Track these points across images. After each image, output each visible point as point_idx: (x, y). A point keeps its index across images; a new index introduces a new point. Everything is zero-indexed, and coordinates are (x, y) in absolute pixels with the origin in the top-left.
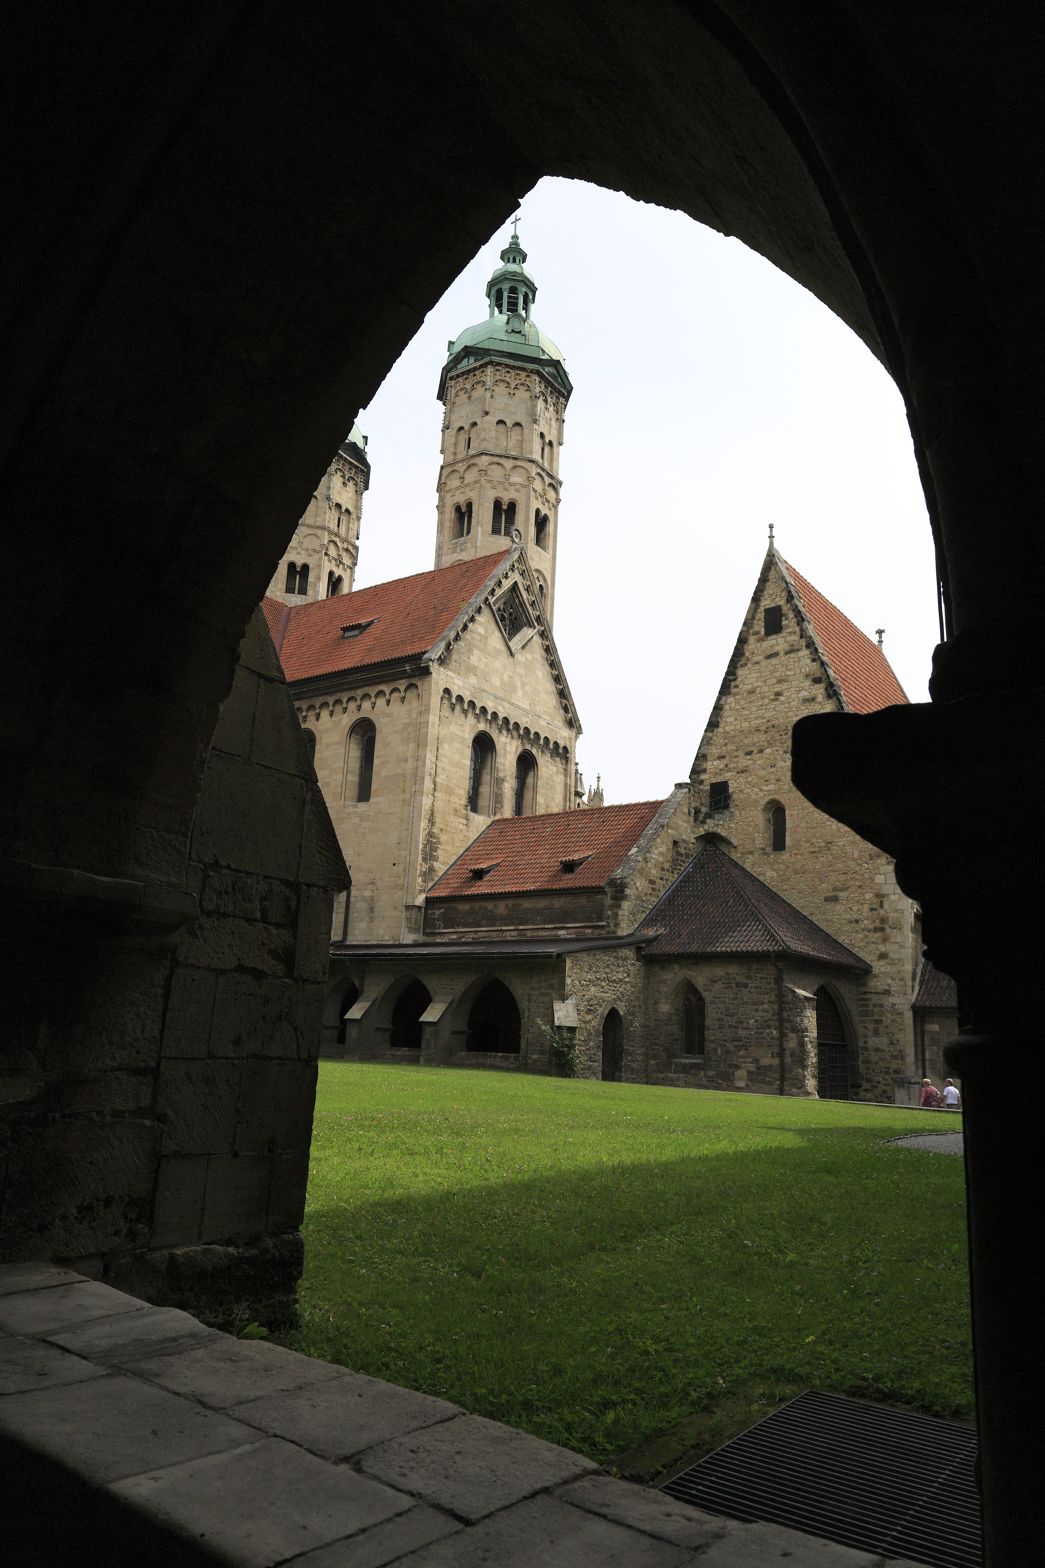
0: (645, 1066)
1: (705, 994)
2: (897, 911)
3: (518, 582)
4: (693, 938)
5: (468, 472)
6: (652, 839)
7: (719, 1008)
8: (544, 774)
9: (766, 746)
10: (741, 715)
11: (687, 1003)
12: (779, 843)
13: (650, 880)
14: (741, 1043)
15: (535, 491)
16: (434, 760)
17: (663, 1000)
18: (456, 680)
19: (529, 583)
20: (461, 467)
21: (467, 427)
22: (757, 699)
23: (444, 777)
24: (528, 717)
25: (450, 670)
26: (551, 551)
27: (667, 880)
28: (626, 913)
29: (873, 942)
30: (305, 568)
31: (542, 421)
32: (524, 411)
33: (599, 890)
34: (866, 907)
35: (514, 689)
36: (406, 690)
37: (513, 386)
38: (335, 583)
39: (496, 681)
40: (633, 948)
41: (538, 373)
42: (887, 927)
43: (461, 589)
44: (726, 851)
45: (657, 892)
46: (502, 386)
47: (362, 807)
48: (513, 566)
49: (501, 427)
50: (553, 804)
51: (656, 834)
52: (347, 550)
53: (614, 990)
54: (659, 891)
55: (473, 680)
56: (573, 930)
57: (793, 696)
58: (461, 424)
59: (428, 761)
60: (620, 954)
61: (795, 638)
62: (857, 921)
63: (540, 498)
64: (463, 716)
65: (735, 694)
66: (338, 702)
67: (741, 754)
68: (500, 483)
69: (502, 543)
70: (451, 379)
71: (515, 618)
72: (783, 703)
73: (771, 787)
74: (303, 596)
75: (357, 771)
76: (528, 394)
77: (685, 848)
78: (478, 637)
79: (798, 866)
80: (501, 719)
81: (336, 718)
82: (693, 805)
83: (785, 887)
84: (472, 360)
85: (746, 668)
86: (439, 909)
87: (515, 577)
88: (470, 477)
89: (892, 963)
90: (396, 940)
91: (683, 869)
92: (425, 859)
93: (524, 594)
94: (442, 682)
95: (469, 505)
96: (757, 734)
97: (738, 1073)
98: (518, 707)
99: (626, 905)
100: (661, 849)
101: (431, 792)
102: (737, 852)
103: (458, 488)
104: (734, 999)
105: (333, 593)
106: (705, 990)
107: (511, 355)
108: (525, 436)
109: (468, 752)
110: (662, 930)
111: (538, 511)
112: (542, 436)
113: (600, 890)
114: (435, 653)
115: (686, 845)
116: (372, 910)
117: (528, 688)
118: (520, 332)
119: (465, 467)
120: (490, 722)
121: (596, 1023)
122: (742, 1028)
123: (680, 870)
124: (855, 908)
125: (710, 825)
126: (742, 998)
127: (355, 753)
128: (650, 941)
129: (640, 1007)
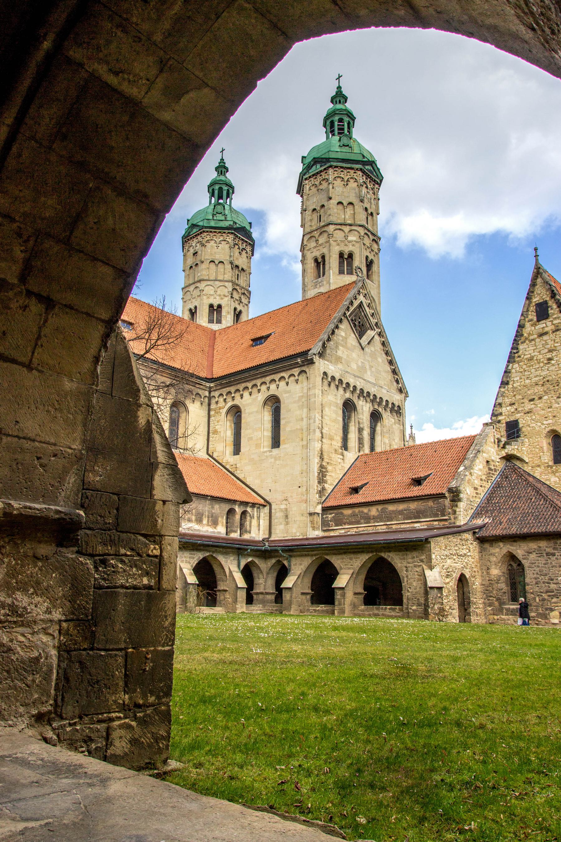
0: (485, 611)
1: (523, 562)
3: (363, 301)
4: (511, 524)
5: (321, 237)
6: (473, 461)
7: (535, 570)
8: (387, 424)
9: (544, 394)
10: (524, 375)
11: (510, 568)
14: (553, 594)
16: (320, 418)
17: (493, 566)
19: (369, 302)
20: (316, 234)
21: (318, 208)
22: (535, 364)
23: (327, 429)
25: (326, 360)
26: (377, 283)
28: (462, 510)
30: (220, 306)
31: (366, 200)
32: (354, 195)
33: (441, 496)
35: (366, 372)
36: (299, 375)
37: (346, 180)
38: (238, 315)
39: (354, 366)
40: (471, 532)
41: (361, 170)
43: (327, 309)
44: (520, 466)
46: (339, 180)
47: (275, 451)
48: (359, 291)
49: (340, 207)
50: (394, 443)
51: (476, 456)
52: (244, 294)
55: (340, 366)
56: (425, 523)
58: (314, 207)
59: (317, 419)
60: (463, 537)
64: (336, 389)
65: (518, 363)
66: (255, 385)
67: (526, 401)
69: (348, 279)
70: (306, 179)
72: (553, 365)
73: (550, 421)
74: (219, 324)
75: (270, 429)
76: (356, 184)
77: (494, 466)
78: (341, 338)
81: (253, 396)
84: (318, 166)
86: (331, 514)
88: (322, 240)
90: (303, 536)
91: (493, 479)
92: (319, 483)
93: (367, 309)
95: (323, 257)
96: (537, 387)
97: (553, 614)
99: (462, 505)
100: (479, 467)
101: (320, 439)
102: (528, 466)
103: (315, 247)
104: (545, 564)
105: (237, 322)
107: (343, 161)
108: (356, 211)
109: (340, 412)
110: (487, 520)
111: (367, 257)
112: (366, 209)
114: (317, 348)
116: (287, 517)
117: (373, 369)
118: (348, 146)
119: (318, 234)
121: (452, 584)
122: (553, 583)
126: (551, 563)
127: (267, 417)
128: (481, 528)
129: (478, 572)
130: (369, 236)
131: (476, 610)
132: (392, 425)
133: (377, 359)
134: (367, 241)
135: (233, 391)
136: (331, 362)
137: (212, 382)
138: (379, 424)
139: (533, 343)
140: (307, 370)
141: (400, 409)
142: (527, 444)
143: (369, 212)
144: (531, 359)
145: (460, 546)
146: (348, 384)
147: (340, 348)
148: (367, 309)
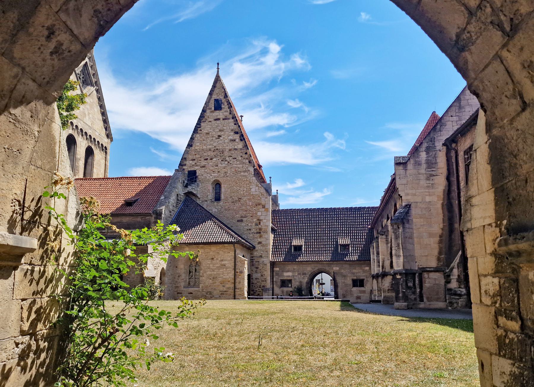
2: (266, 226)
12: (218, 198)
19: (92, 64)
29: (256, 238)
34: (254, 224)
42: (261, 232)
57: (226, 138)
61: (227, 114)
62: (250, 230)
67: (202, 159)
72: (221, 140)
79: (227, 207)
83: (221, 216)
85: (205, 123)
89: (263, 246)
98: (87, 125)
102: (199, 200)
117: (91, 116)
124: (249, 225)
125: (190, 189)
139: (210, 123)
142: (200, 186)
144: (208, 134)
148: (90, 68)
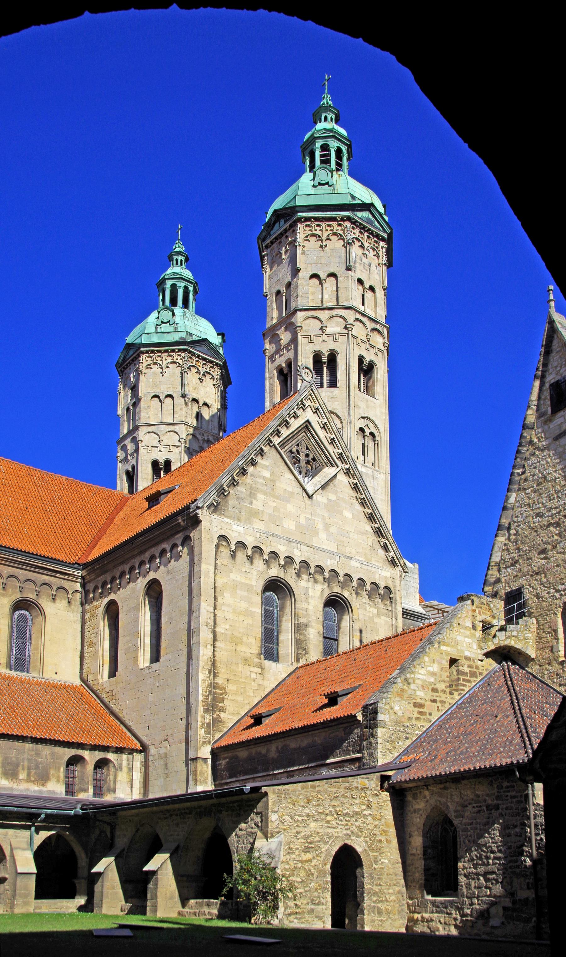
1: (456, 822)
3: (311, 420)
8: (361, 617)
13: (414, 703)
15: (355, 337)
18: (235, 527)
23: (227, 627)
24: (334, 559)
25: (227, 517)
27: (442, 702)
35: (316, 532)
45: (428, 716)
53: (347, 825)
54: (430, 714)
55: (258, 525)
60: (355, 784)
63: (361, 344)
64: (247, 563)
68: (317, 336)
71: (314, 459)
78: (261, 481)
80: (298, 563)
82: (480, 618)
87: (308, 415)
94: (215, 529)
100: (430, 669)
106: (456, 817)
110: (422, 756)
113: (354, 719)
115: (471, 663)
117: (333, 529)
120: (284, 567)
123: (463, 690)
130: (364, 324)
131: (379, 905)
132: (371, 618)
133: (341, 513)
134: (359, 330)
135: (109, 579)
136: (239, 520)
137: (83, 569)
138: (346, 618)
140: (192, 535)
141: (391, 592)
143: (367, 285)
145: (346, 801)
146: (274, 555)
147: (260, 496)
